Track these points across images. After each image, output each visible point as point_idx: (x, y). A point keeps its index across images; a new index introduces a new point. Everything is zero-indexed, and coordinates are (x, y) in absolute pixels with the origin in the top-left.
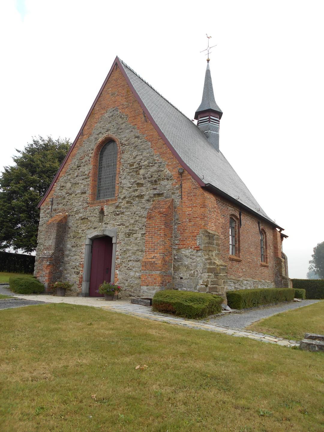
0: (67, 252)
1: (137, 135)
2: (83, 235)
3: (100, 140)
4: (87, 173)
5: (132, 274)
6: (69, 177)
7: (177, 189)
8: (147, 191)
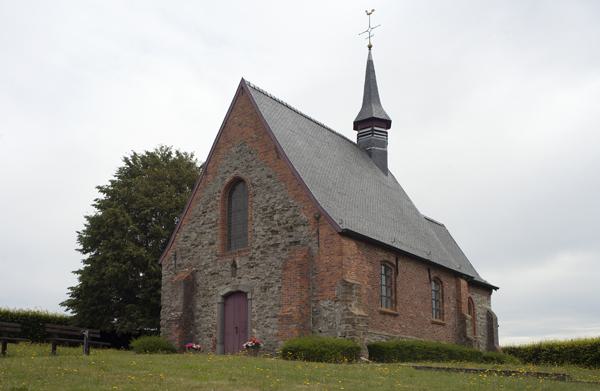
0: (198, 313)
1: (270, 174)
3: (227, 180)
4: (214, 220)
5: (270, 331)
6: (194, 225)
7: (314, 236)
8: (282, 239)
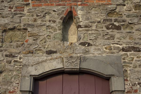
2: (8, 67)
